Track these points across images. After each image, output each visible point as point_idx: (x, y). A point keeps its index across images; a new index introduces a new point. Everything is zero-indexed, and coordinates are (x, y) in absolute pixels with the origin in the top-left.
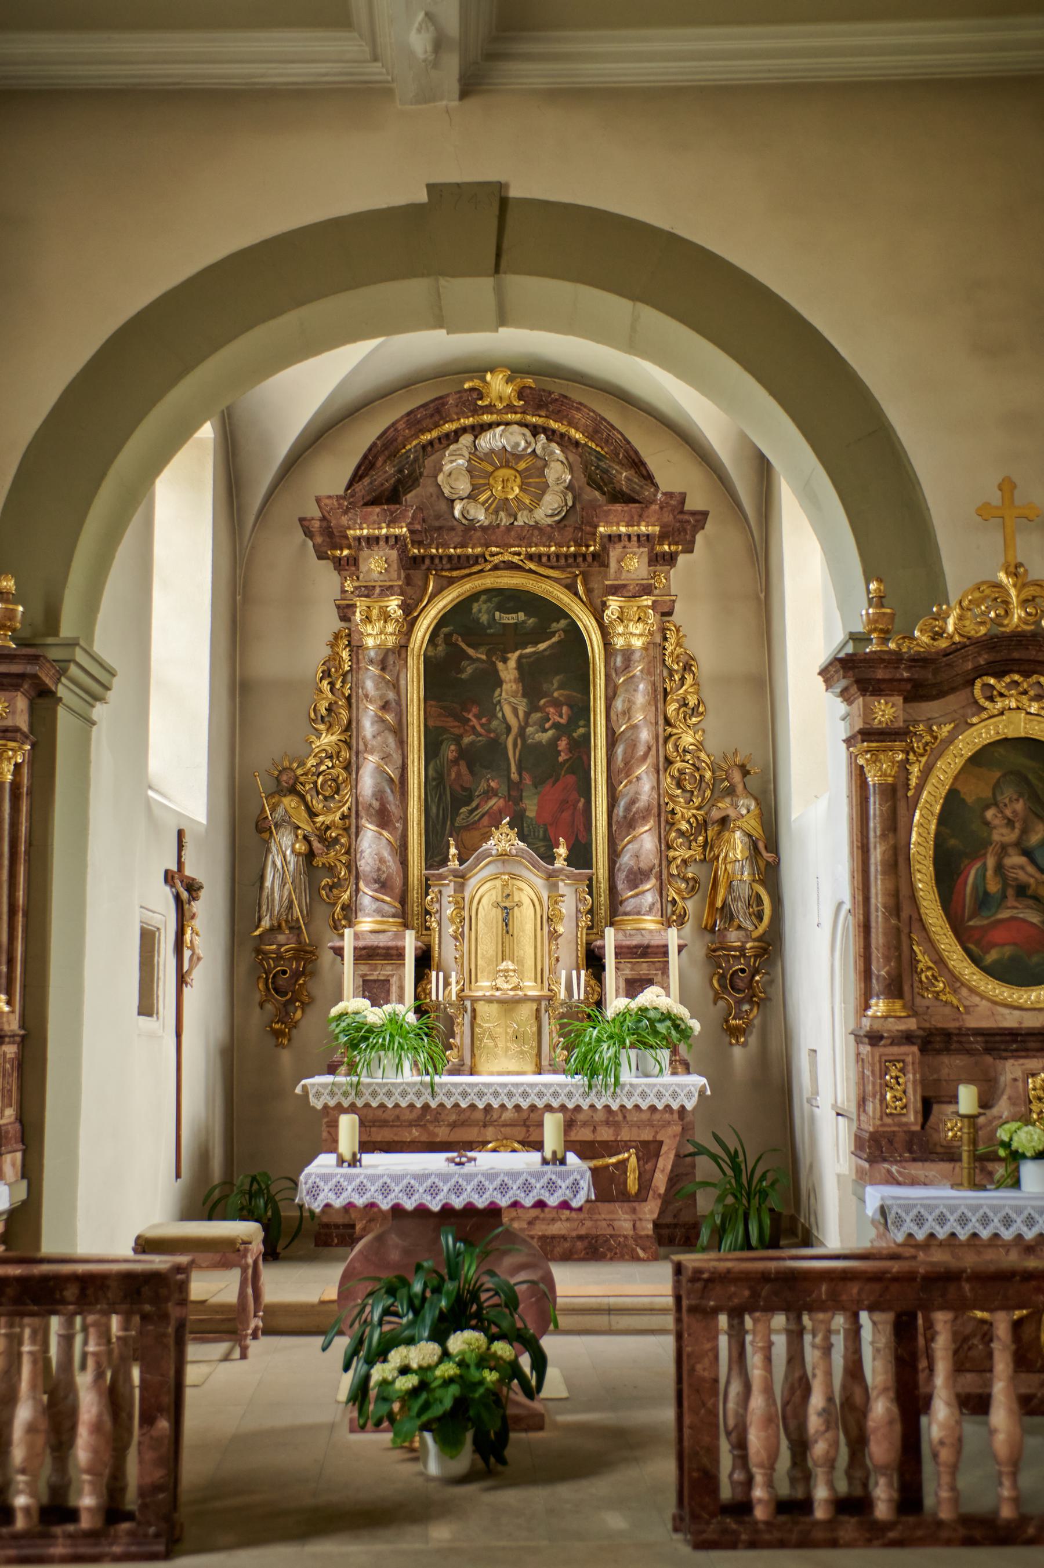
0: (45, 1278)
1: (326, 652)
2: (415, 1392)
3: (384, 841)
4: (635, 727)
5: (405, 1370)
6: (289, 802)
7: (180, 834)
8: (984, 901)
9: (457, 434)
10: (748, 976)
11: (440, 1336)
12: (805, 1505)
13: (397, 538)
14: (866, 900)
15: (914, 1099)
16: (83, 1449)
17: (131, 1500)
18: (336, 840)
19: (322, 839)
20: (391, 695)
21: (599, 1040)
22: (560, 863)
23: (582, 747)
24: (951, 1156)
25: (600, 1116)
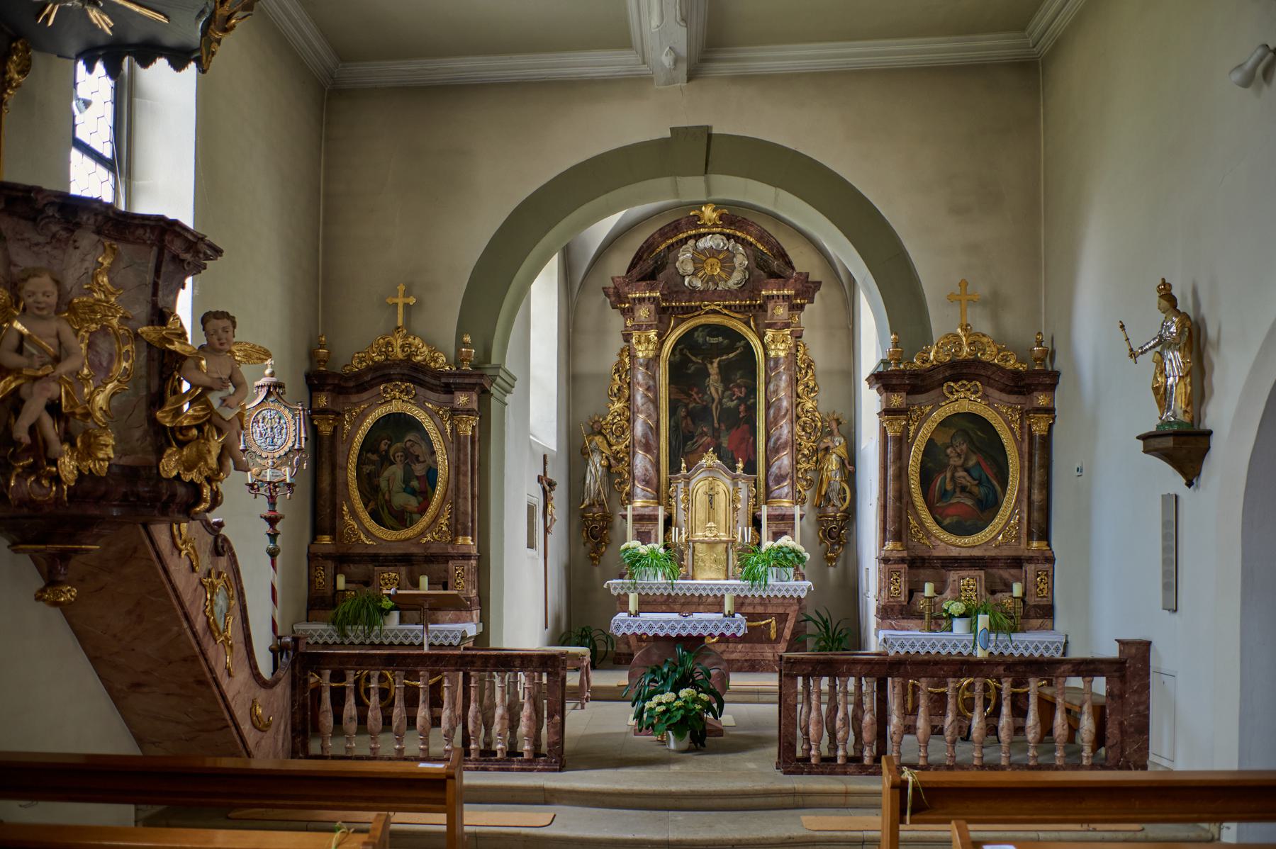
0: (507, 656)
1: (618, 358)
2: (664, 713)
4: (780, 399)
5: (660, 704)
6: (598, 439)
7: (545, 457)
8: (944, 494)
10: (837, 532)
11: (676, 689)
12: (834, 759)
14: (886, 493)
15: (904, 590)
16: (523, 728)
17: (544, 748)
18: (622, 459)
19: (615, 459)
20: (651, 383)
21: (757, 563)
22: (739, 472)
23: (752, 409)
24: (920, 616)
25: (757, 601)
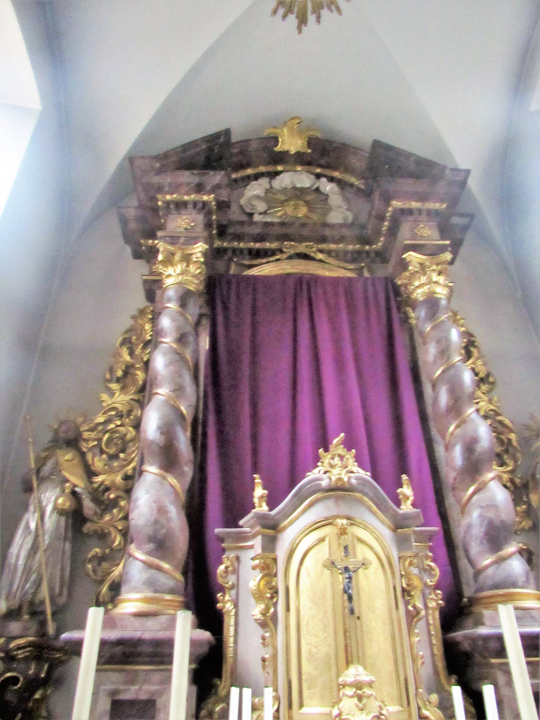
3: (169, 488)
6: (67, 456)
9: (257, 177)
13: (205, 204)
22: (407, 508)
